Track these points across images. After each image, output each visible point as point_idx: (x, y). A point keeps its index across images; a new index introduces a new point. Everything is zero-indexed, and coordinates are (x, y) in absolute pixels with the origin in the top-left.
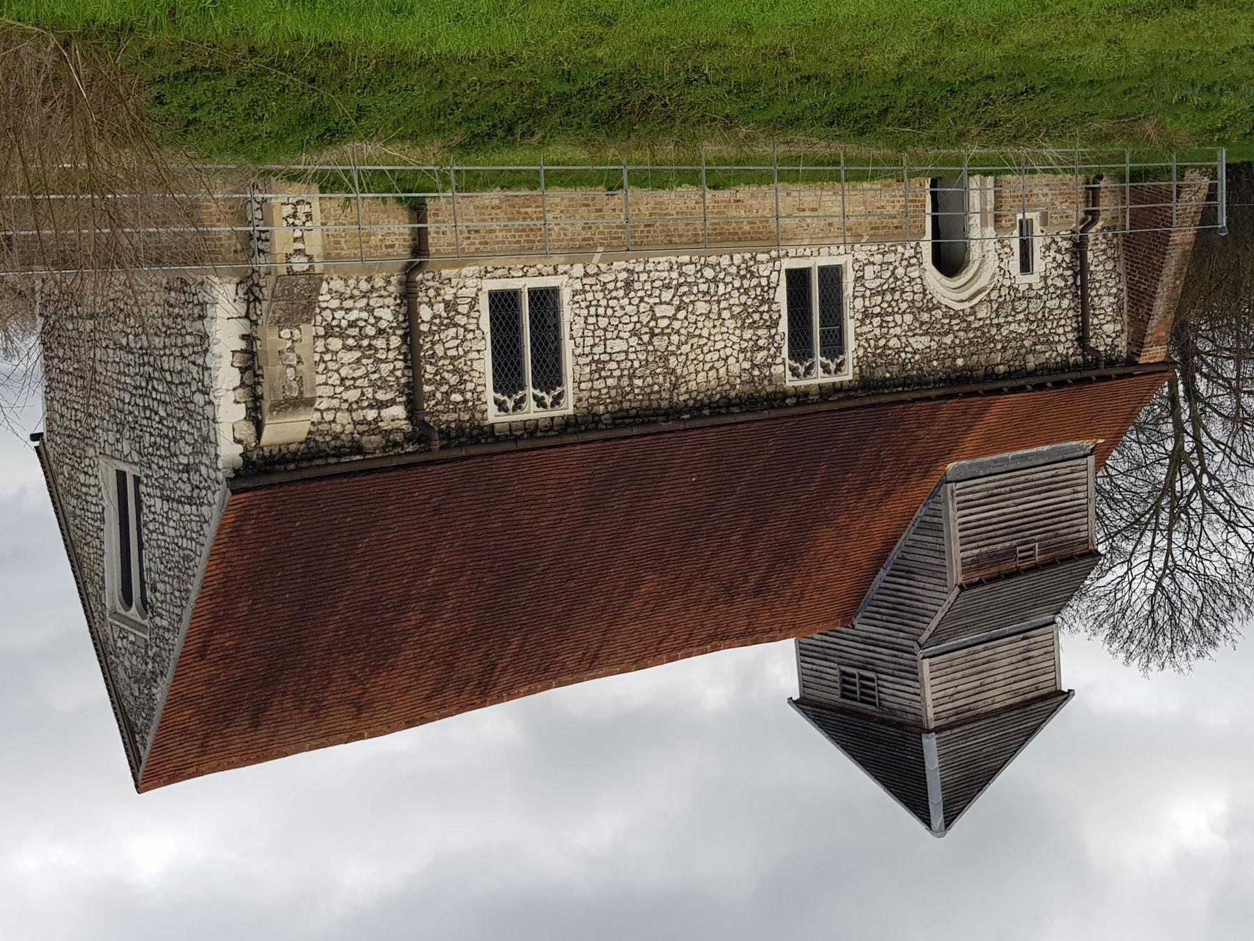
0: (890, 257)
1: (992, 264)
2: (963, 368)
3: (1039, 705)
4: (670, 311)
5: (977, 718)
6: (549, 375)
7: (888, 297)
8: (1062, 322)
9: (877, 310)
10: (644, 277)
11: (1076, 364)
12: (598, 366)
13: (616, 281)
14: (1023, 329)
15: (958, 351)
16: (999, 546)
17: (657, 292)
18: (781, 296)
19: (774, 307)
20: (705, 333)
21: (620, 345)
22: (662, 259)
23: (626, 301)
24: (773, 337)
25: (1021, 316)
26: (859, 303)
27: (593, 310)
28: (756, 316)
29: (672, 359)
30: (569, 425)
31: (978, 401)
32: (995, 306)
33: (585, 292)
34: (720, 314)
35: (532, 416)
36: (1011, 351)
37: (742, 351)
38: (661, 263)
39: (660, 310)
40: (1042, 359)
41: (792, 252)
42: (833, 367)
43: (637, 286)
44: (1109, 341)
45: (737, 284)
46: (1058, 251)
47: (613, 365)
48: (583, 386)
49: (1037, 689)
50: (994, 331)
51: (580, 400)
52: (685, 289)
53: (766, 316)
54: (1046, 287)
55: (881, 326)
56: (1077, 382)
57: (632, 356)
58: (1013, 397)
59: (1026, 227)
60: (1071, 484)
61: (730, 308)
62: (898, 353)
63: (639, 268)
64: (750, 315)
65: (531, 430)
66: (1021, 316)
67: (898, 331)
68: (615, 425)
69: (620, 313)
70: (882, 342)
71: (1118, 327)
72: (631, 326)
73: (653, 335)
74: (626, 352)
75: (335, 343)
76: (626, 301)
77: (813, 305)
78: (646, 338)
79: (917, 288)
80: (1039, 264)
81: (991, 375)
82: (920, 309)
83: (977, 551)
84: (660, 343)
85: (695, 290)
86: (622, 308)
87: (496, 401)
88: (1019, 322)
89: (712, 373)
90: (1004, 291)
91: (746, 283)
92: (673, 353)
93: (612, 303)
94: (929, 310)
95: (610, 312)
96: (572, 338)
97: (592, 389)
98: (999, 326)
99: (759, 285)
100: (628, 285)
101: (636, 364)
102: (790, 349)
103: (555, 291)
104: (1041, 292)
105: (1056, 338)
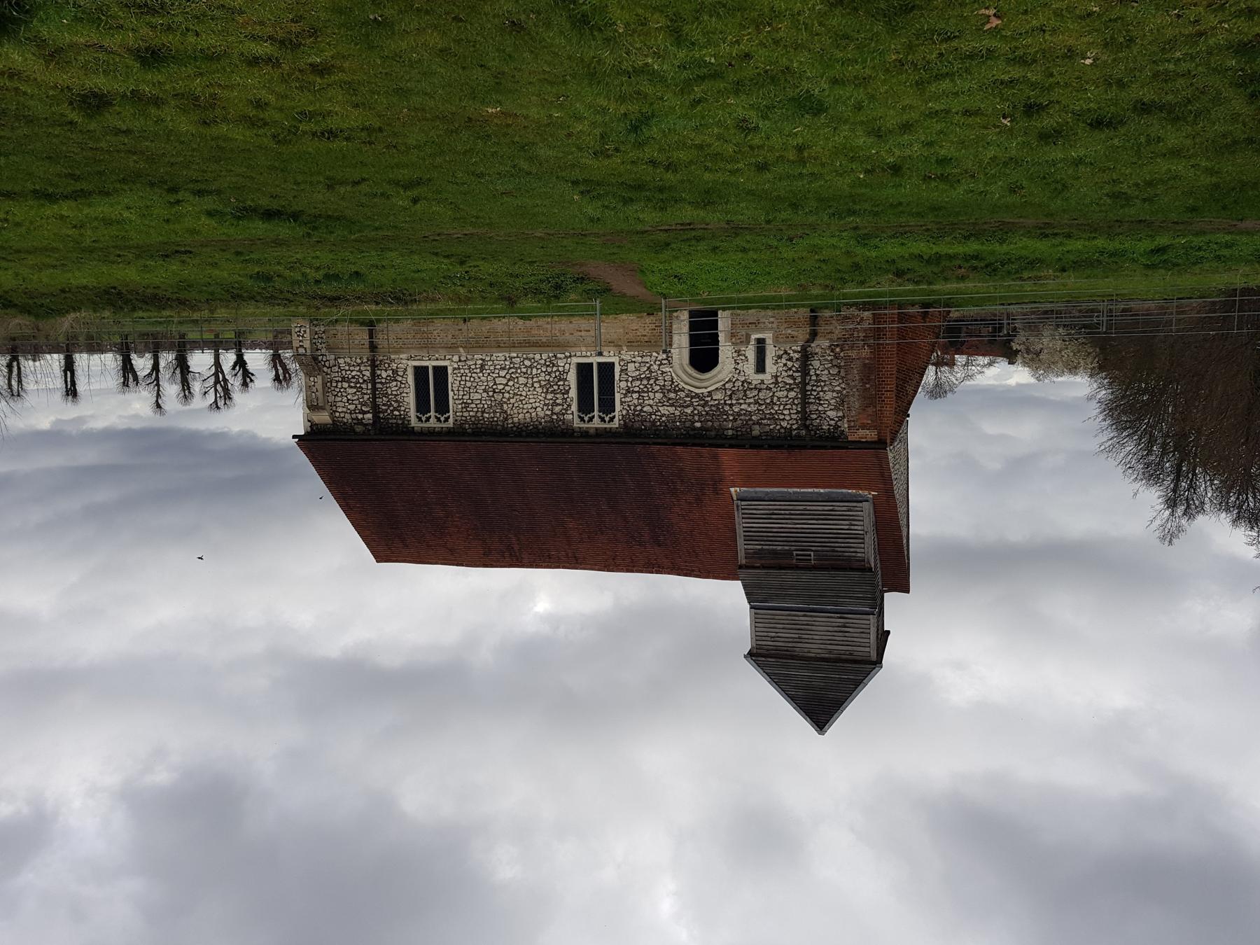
0: (648, 359)
4: (504, 381)
6: (443, 407)
7: (645, 382)
14: (753, 408)
18: (572, 378)
21: (477, 396)
26: (623, 384)
30: (450, 432)
31: (704, 451)
37: (547, 405)
38: (500, 355)
39: (498, 381)
41: (579, 354)
50: (727, 408)
60: (851, 520)
65: (431, 433)
67: (651, 402)
70: (639, 408)
75: (346, 385)
77: (596, 384)
82: (669, 391)
88: (749, 404)
90: (739, 384)
94: (676, 392)
98: (731, 405)
100: (482, 368)
103: (445, 368)
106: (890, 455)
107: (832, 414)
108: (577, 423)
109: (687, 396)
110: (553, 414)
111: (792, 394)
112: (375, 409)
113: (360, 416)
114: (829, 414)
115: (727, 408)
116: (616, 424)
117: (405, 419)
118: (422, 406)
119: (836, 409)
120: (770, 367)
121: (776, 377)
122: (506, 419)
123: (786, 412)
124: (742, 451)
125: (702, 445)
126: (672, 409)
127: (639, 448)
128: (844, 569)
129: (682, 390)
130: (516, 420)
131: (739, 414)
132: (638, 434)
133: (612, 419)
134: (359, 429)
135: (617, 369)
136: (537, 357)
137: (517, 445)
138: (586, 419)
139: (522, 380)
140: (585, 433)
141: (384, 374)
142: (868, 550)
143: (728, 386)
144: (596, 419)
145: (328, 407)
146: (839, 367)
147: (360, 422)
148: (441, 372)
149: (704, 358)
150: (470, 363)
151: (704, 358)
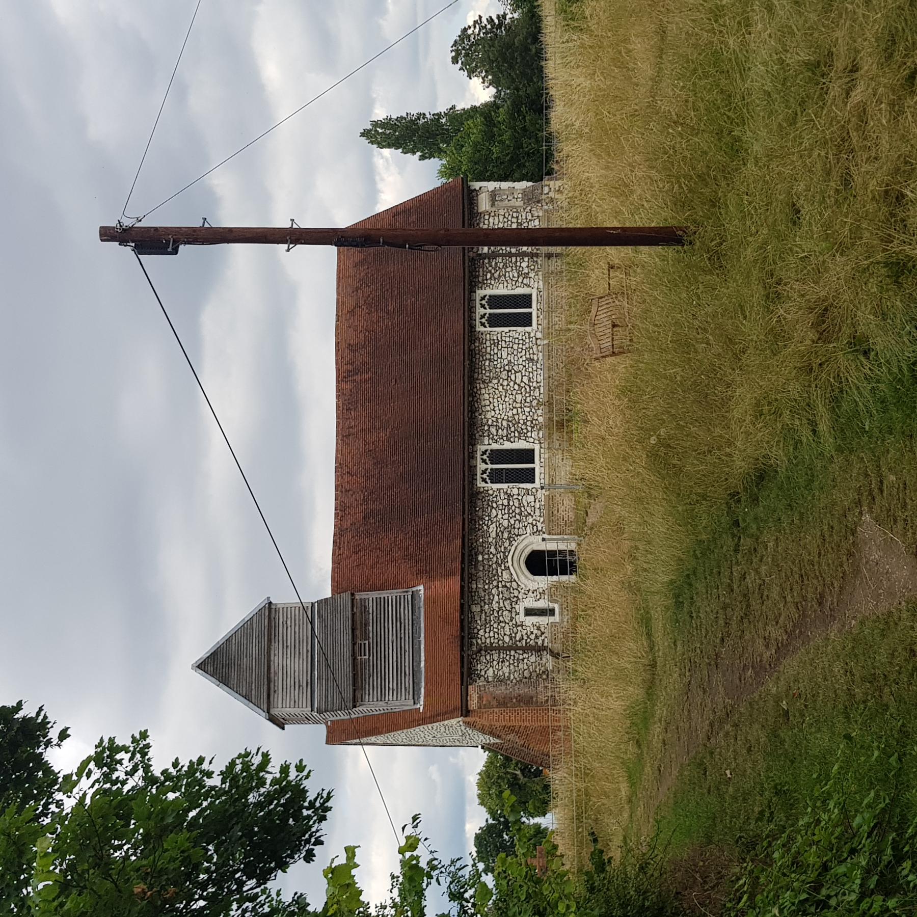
0: (537, 513)
2: (477, 561)
3: (266, 686)
4: (518, 381)
5: (270, 640)
6: (495, 321)
7: (517, 511)
8: (496, 636)
9: (511, 503)
10: (534, 367)
11: (472, 644)
12: (496, 344)
13: (534, 354)
14: (495, 606)
15: (486, 556)
16: (371, 628)
18: (521, 445)
20: (507, 399)
23: (524, 358)
25: (502, 605)
26: (515, 491)
28: (513, 429)
29: (496, 381)
30: (472, 327)
31: (458, 565)
32: (508, 585)
35: (477, 311)
36: (483, 594)
40: (477, 618)
41: (542, 450)
43: (531, 364)
44: (483, 673)
45: (529, 418)
46: (537, 637)
47: (496, 351)
49: (275, 692)
50: (495, 583)
52: (528, 390)
54: (517, 626)
56: (462, 638)
59: (552, 612)
63: (539, 366)
64: (514, 425)
65: (471, 310)
66: (502, 605)
68: (470, 350)
69: (519, 355)
70: (495, 505)
71: (490, 679)
73: (508, 371)
76: (524, 358)
77: (516, 466)
78: (507, 368)
80: (530, 620)
81: (472, 578)
82: (510, 532)
83: (371, 611)
84: (504, 375)
88: (498, 602)
89: (488, 403)
91: (529, 423)
94: (509, 538)
98: (497, 587)
102: (497, 450)
104: (514, 622)
105: (487, 630)
106: (454, 722)
108: (481, 448)
109: (505, 548)
115: (495, 583)
116: (480, 484)
117: (484, 284)
118: (496, 301)
122: (484, 382)
124: (458, 596)
125: (463, 562)
126: (493, 535)
127: (459, 505)
128: (354, 685)
130: (483, 391)
131: (490, 593)
132: (472, 503)
133: (484, 480)
135: (529, 486)
136: (540, 412)
137: (460, 393)
138: (485, 457)
139: (519, 398)
140: (472, 456)
141: (524, 265)
142: (371, 707)
143: (514, 583)
144: (484, 466)
145: (493, 209)
146: (530, 678)
148: (526, 320)
149: (538, 563)
150: (535, 347)
151: (538, 563)
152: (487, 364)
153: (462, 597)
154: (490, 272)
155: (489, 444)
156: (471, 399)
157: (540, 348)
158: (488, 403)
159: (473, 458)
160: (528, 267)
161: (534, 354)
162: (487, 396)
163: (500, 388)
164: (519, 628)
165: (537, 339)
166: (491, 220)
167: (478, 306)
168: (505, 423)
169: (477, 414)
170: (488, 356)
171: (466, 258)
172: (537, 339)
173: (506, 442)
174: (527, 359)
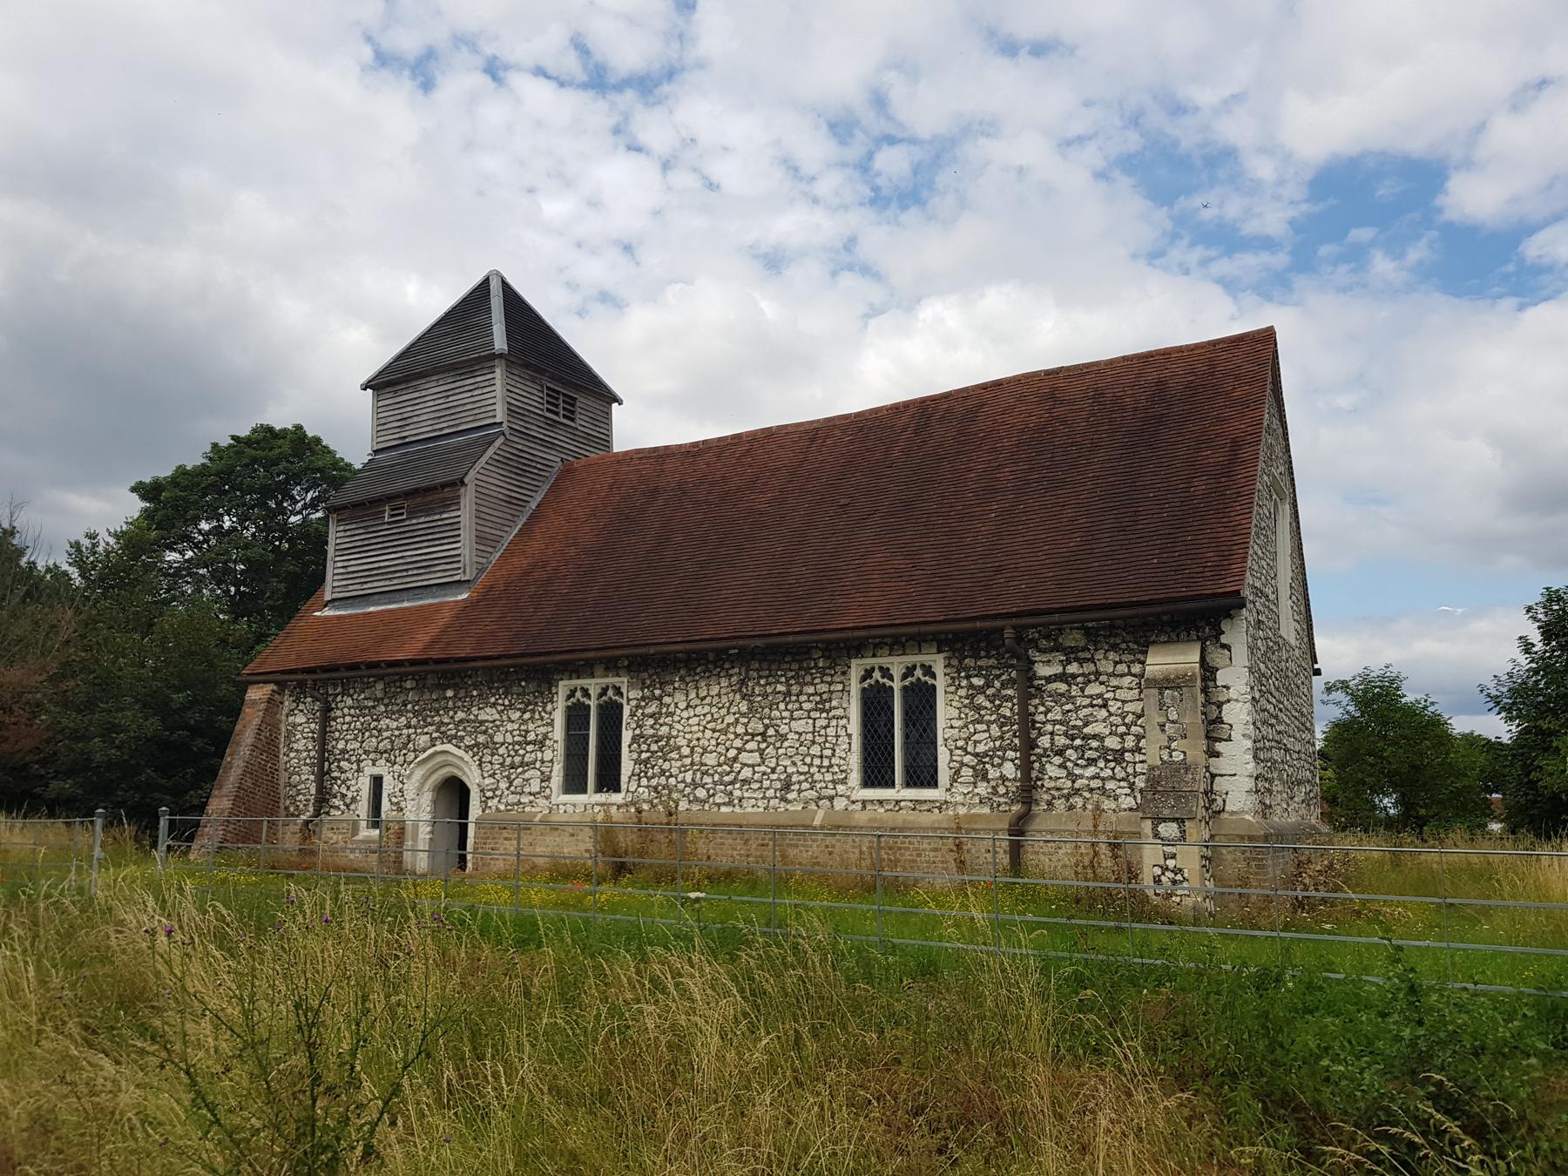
0: (512, 799)
1: (410, 787)
4: (744, 757)
7: (517, 759)
9: (530, 748)
10: (770, 793)
12: (822, 705)
13: (800, 791)
14: (384, 722)
17: (757, 776)
18: (627, 766)
19: (635, 756)
20: (708, 734)
21: (798, 726)
22: (750, 810)
23: (790, 770)
24: (638, 726)
25: (386, 734)
26: (548, 755)
27: (826, 763)
28: (654, 747)
29: (744, 707)
30: (857, 648)
33: (833, 781)
34: (692, 752)
39: (756, 758)
42: (578, 694)
45: (672, 781)
47: (806, 706)
48: (840, 687)
51: (844, 673)
52: (726, 779)
53: (644, 747)
55: (527, 732)
57: (786, 714)
58: (400, 656)
61: (681, 757)
62: (511, 705)
65: (897, 644)
66: (386, 734)
67: (510, 727)
69: (797, 759)
70: (527, 715)
72: (786, 744)
73: (763, 734)
74: (792, 719)
76: (790, 770)
77: (595, 758)
78: (771, 732)
79: (487, 767)
85: (716, 777)
86: (794, 764)
87: (934, 676)
88: (388, 728)
90: (400, 759)
91: (663, 780)
92: (743, 715)
93: (806, 769)
94: (477, 745)
95: (808, 760)
96: (849, 736)
97: (830, 684)
99: (649, 779)
101: (782, 706)
107: (300, 719)
108: (623, 681)
110: (660, 698)
111: (341, 745)
112: (1029, 687)
113: (1073, 668)
114: (300, 720)
116: (563, 687)
117: (958, 670)
118: (921, 701)
119: (295, 725)
120: (364, 784)
121: (358, 771)
122: (743, 682)
123: (348, 719)
129: (468, 748)
134: (1073, 639)
139: (710, 759)
140: (611, 666)
143: (411, 756)
147: (1071, 654)
148: (876, 772)
152: (780, 688)
153: (390, 664)
154: (988, 685)
155: (629, 700)
156: (711, 656)
157: (813, 806)
158: (703, 693)
159: (607, 669)
160: (1003, 778)
161: (800, 791)
162: (715, 690)
163: (730, 719)
164: (355, 766)
165: (831, 799)
166: (1128, 679)
167: (910, 659)
168: (665, 729)
169: (682, 672)
170: (795, 689)
171: (999, 623)
172: (831, 799)
173: (630, 733)
174: (789, 776)
